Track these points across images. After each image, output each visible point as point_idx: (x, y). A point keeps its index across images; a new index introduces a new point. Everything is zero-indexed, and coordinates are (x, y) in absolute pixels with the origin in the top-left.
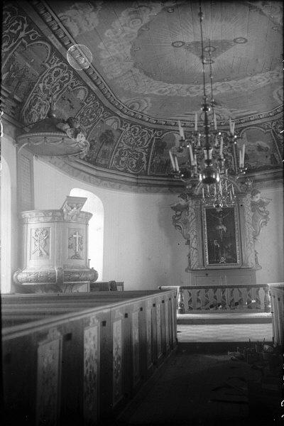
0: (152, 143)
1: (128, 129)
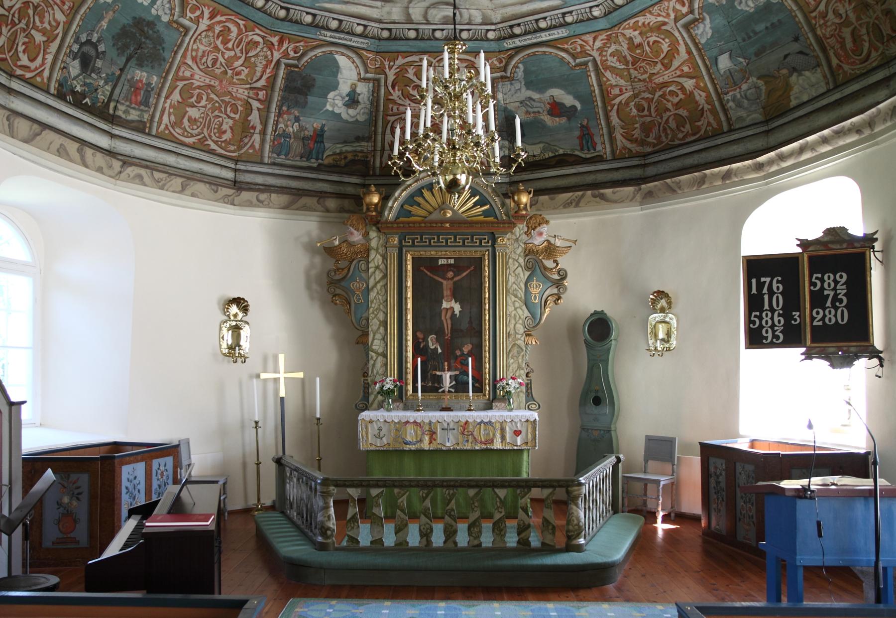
0: (274, 77)
1: (205, 23)
